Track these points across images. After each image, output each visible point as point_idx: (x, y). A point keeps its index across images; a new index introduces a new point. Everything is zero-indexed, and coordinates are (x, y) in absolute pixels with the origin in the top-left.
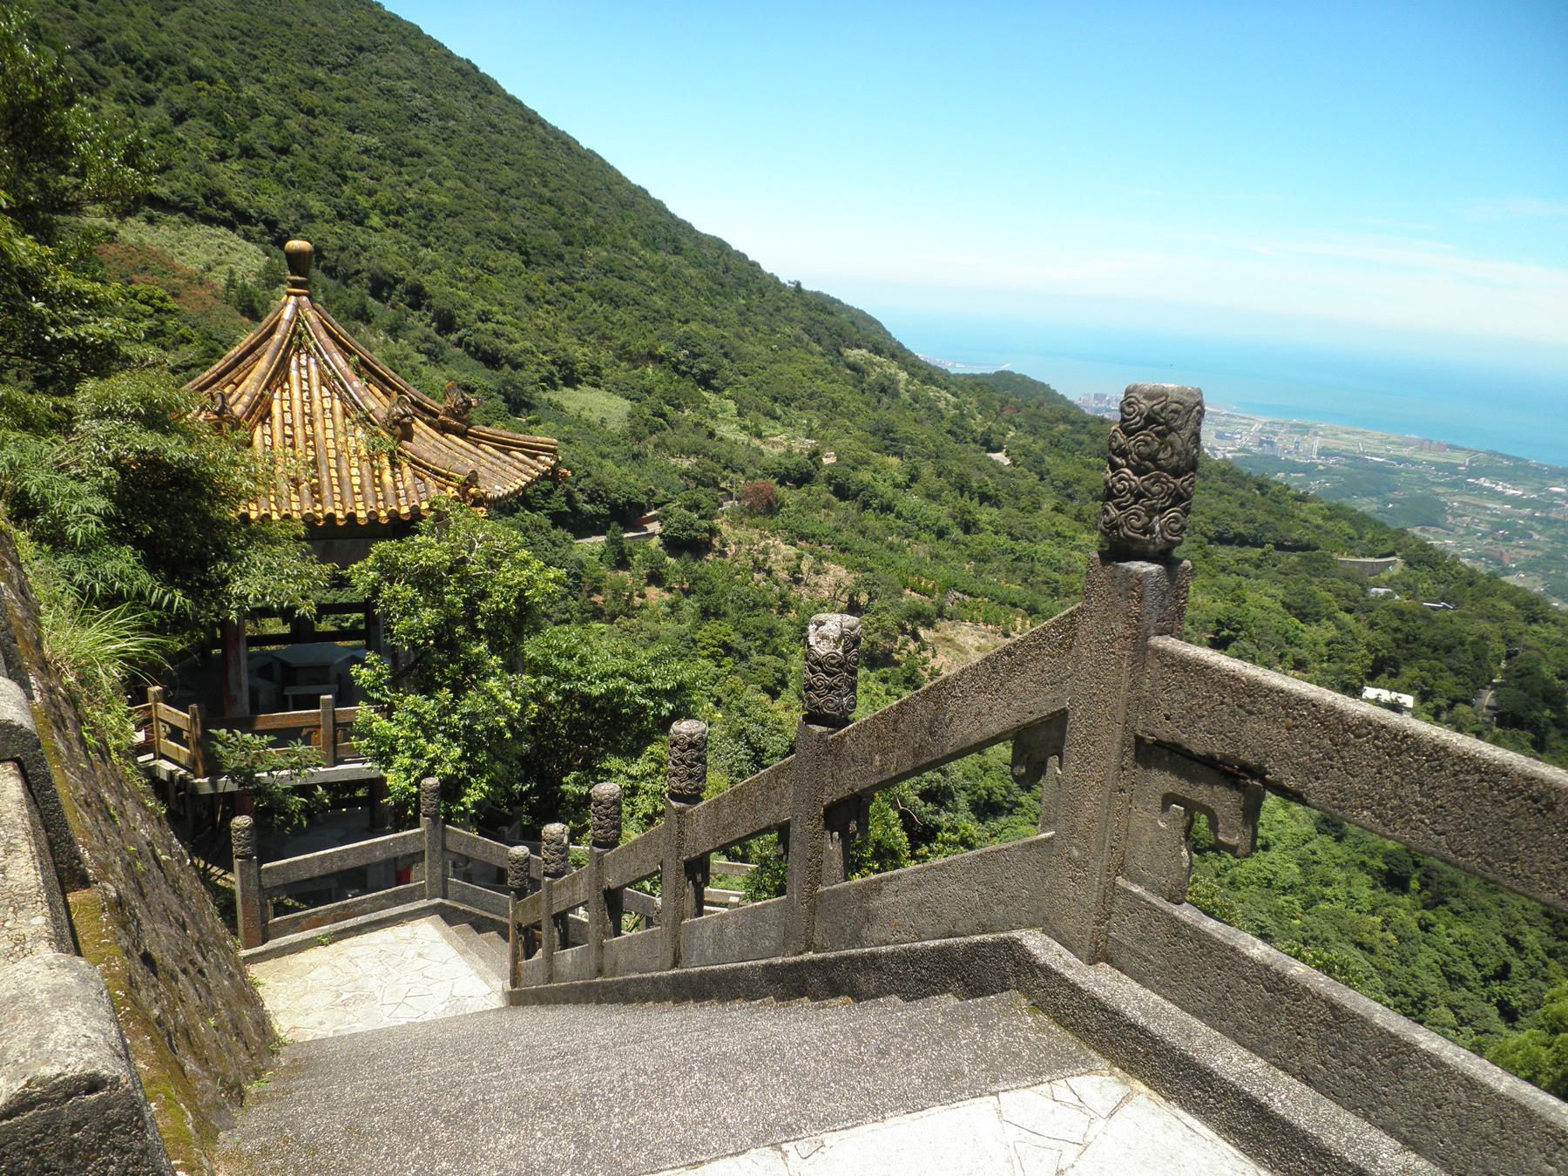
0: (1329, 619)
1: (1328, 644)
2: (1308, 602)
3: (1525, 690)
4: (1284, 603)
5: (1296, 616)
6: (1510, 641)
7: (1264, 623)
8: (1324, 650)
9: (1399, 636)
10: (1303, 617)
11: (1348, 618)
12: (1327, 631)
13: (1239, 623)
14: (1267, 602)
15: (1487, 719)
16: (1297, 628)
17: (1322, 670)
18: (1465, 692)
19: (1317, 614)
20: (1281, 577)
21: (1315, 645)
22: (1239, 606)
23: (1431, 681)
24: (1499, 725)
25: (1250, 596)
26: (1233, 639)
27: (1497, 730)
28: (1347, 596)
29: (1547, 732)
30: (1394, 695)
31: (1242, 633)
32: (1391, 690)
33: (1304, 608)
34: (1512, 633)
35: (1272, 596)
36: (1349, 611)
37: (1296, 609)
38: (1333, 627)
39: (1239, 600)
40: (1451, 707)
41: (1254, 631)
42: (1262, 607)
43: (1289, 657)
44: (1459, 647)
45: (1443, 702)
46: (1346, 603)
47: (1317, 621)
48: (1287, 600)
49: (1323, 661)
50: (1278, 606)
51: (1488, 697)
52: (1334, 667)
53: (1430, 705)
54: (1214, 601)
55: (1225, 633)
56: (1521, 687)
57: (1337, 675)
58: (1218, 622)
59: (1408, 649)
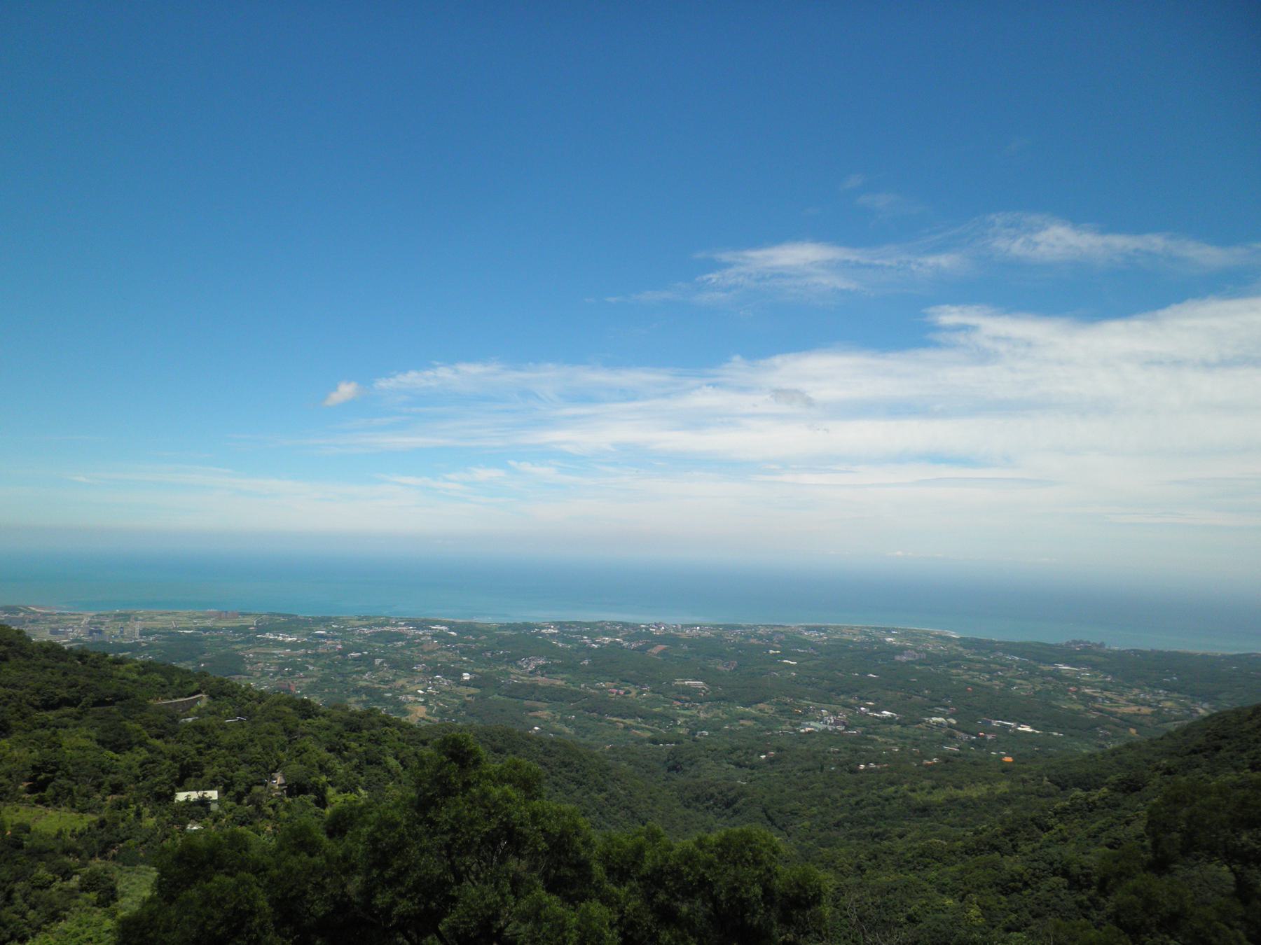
0: (141, 746)
1: (141, 766)
2: (120, 735)
3: (305, 764)
4: (99, 741)
5: (111, 749)
6: (290, 732)
7: (79, 760)
8: (138, 771)
9: (201, 745)
10: (117, 748)
11: (158, 742)
12: (144, 754)
13: (53, 764)
14: (84, 743)
15: (279, 793)
16: (112, 759)
17: (138, 789)
18: (259, 777)
19: (130, 743)
20: (97, 722)
21: (130, 768)
22: (55, 751)
23: (230, 774)
24: (290, 794)
25: (66, 742)
26: (51, 780)
27: (287, 800)
28: (156, 726)
29: (324, 791)
30: (200, 793)
31: (58, 773)
32: (197, 790)
33: (117, 740)
34: (290, 726)
35: (88, 737)
36: (158, 737)
37: (109, 743)
38: (145, 751)
39: (56, 745)
40: (249, 790)
41: (71, 769)
42: (78, 748)
43: (106, 784)
44: (250, 744)
45: (241, 788)
46: (155, 731)
47: (129, 750)
48: (101, 738)
49: (139, 782)
50: (95, 745)
51: (279, 779)
52: (147, 783)
53: (231, 793)
54: (31, 752)
55: (42, 777)
56: (301, 762)
57: (151, 788)
58: (34, 767)
59: (209, 754)
